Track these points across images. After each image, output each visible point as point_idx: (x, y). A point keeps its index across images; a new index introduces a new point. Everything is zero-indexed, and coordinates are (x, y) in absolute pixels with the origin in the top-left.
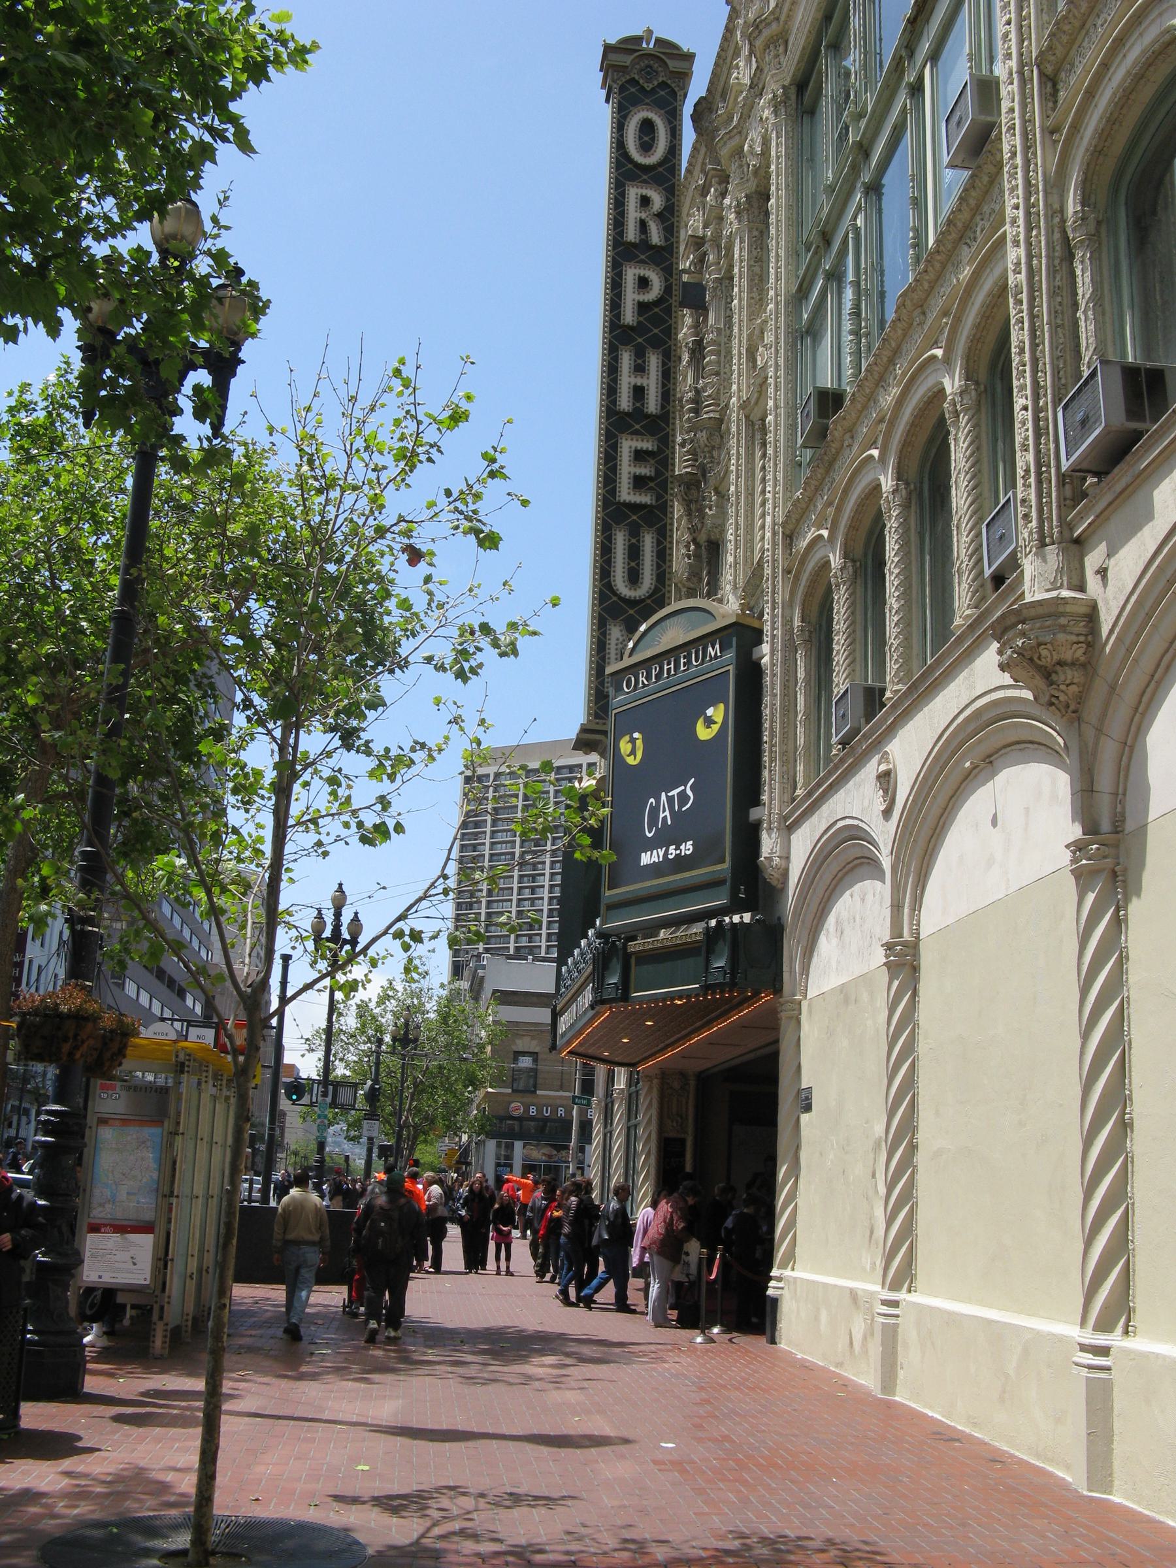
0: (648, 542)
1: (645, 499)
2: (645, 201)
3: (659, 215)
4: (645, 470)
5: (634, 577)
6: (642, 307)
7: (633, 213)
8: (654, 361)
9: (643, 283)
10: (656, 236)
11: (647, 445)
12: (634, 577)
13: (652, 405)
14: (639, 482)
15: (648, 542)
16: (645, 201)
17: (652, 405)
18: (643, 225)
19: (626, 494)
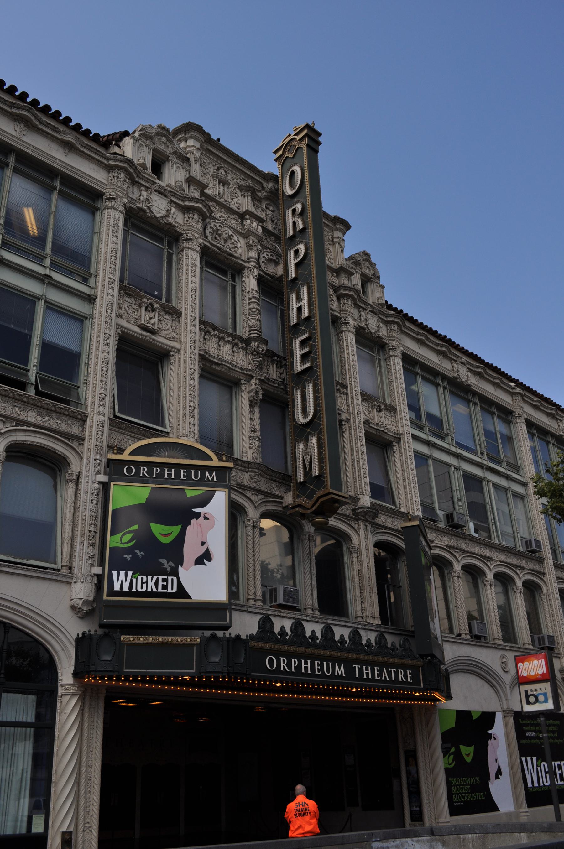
0: (310, 389)
1: (308, 365)
2: (294, 211)
3: (302, 214)
4: (307, 350)
6: (297, 265)
9: (296, 252)
11: (307, 335)
14: (304, 357)
15: (310, 389)
16: (294, 211)
18: (294, 223)
19: (299, 367)
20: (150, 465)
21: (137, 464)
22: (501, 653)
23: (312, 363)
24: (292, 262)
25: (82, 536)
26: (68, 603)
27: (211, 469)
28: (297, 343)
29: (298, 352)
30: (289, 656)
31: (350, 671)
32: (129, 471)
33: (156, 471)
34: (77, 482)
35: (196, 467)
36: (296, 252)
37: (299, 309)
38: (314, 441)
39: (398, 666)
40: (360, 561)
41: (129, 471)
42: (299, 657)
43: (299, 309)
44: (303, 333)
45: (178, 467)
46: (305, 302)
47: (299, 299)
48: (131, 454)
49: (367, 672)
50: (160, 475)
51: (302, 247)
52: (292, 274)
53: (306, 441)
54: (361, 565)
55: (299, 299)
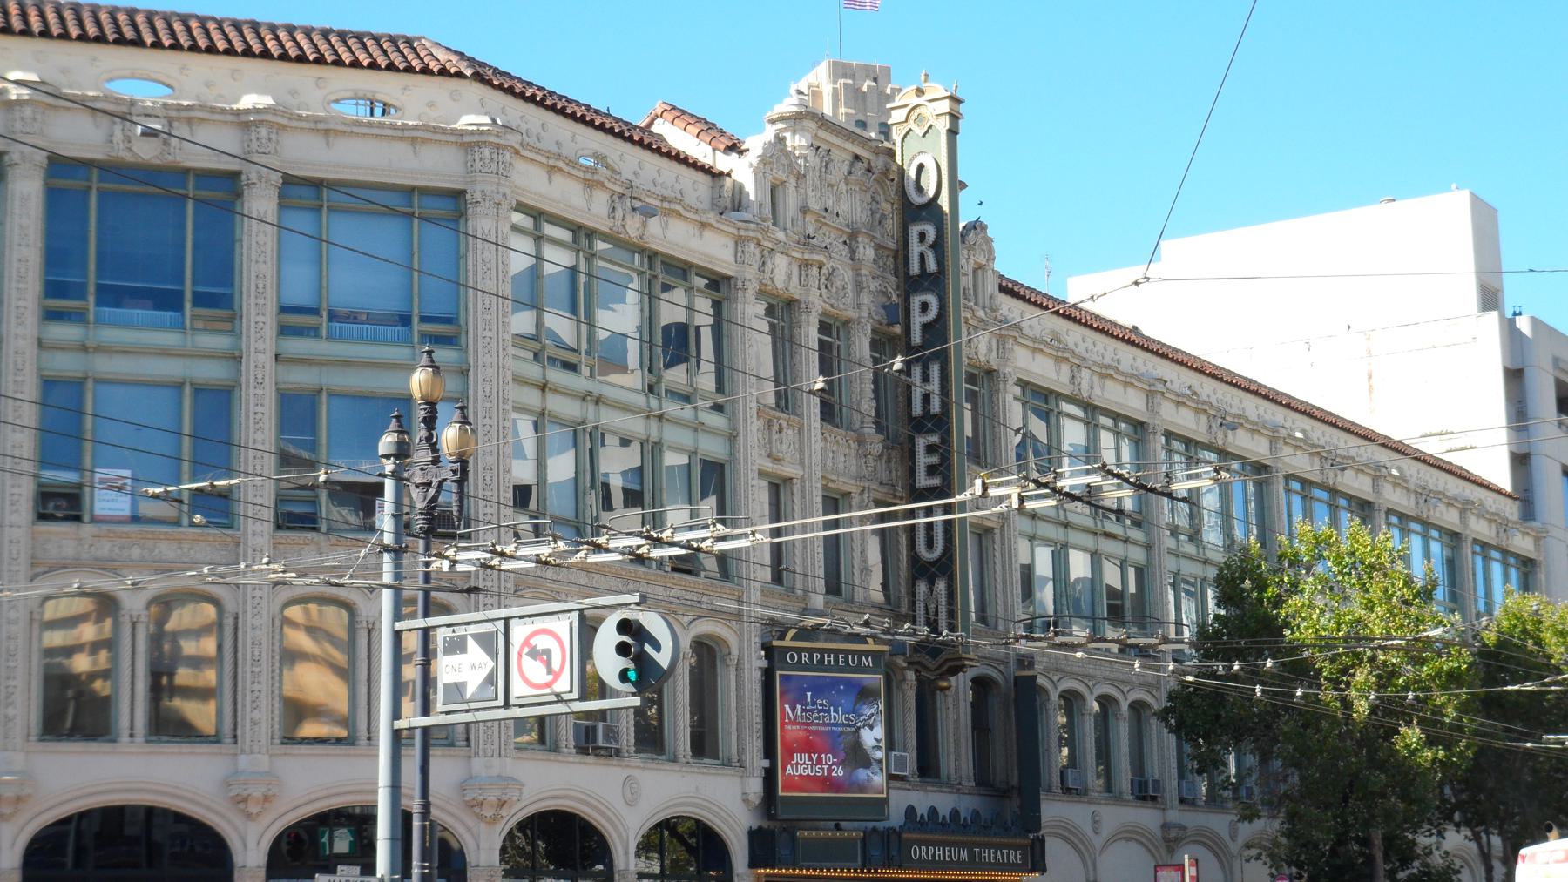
1: (935, 481)
2: (922, 236)
3: (933, 247)
4: (934, 459)
5: (930, 544)
6: (926, 327)
7: (915, 248)
8: (935, 370)
9: (924, 307)
10: (932, 266)
11: (935, 439)
12: (930, 544)
13: (936, 407)
14: (931, 470)
16: (922, 236)
17: (936, 407)
18: (922, 256)
20: (811, 651)
21: (799, 650)
22: (1093, 808)
23: (944, 480)
24: (918, 320)
25: (751, 727)
26: (739, 796)
27: (867, 653)
28: (921, 443)
29: (923, 460)
30: (927, 843)
31: (971, 855)
32: (792, 657)
33: (817, 656)
34: (739, 668)
35: (853, 652)
36: (924, 307)
37: (926, 398)
38: (941, 586)
39: (1009, 847)
40: (956, 706)
41: (792, 657)
42: (935, 844)
43: (926, 398)
44: (930, 431)
45: (836, 652)
46: (934, 386)
47: (926, 379)
48: (793, 639)
49: (985, 854)
50: (821, 661)
51: (932, 300)
52: (917, 338)
53: (931, 584)
54: (958, 714)
55: (926, 379)
